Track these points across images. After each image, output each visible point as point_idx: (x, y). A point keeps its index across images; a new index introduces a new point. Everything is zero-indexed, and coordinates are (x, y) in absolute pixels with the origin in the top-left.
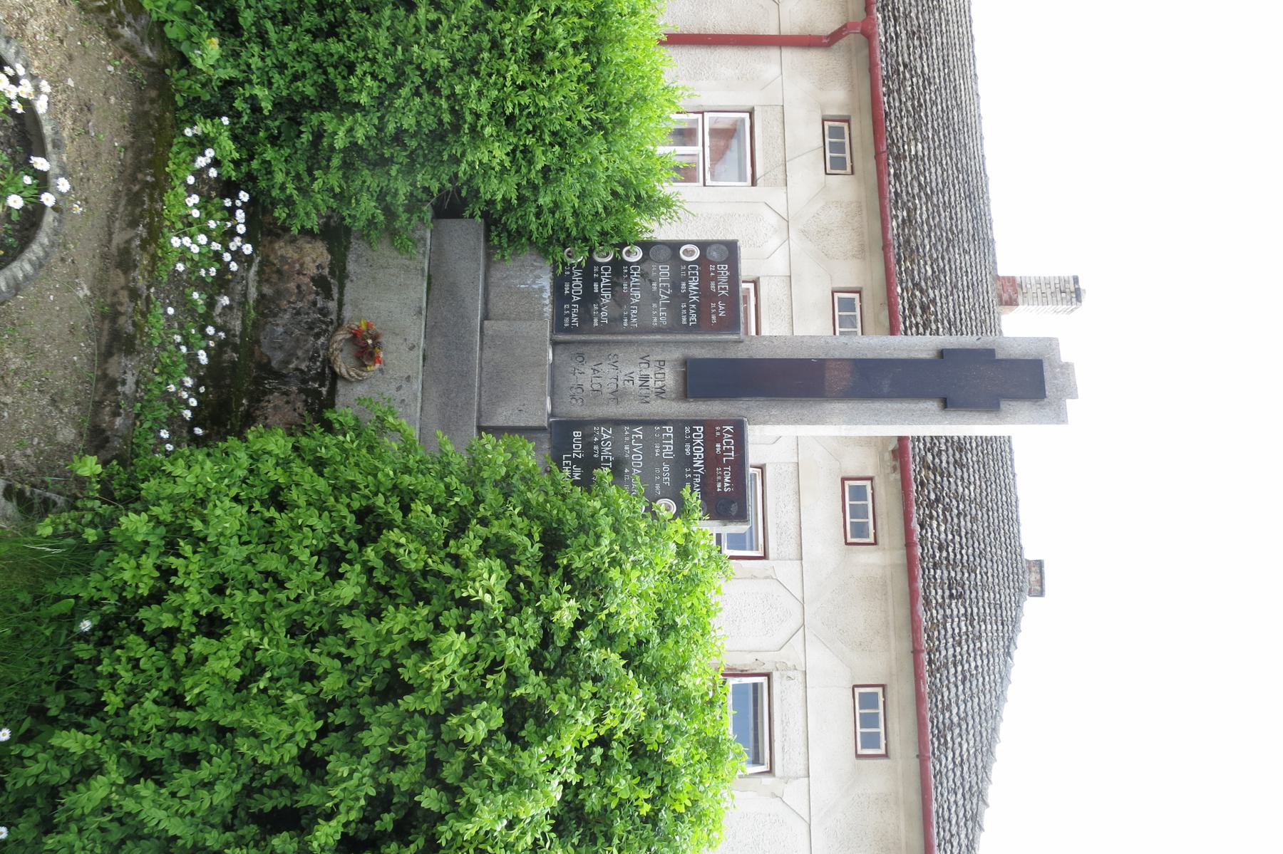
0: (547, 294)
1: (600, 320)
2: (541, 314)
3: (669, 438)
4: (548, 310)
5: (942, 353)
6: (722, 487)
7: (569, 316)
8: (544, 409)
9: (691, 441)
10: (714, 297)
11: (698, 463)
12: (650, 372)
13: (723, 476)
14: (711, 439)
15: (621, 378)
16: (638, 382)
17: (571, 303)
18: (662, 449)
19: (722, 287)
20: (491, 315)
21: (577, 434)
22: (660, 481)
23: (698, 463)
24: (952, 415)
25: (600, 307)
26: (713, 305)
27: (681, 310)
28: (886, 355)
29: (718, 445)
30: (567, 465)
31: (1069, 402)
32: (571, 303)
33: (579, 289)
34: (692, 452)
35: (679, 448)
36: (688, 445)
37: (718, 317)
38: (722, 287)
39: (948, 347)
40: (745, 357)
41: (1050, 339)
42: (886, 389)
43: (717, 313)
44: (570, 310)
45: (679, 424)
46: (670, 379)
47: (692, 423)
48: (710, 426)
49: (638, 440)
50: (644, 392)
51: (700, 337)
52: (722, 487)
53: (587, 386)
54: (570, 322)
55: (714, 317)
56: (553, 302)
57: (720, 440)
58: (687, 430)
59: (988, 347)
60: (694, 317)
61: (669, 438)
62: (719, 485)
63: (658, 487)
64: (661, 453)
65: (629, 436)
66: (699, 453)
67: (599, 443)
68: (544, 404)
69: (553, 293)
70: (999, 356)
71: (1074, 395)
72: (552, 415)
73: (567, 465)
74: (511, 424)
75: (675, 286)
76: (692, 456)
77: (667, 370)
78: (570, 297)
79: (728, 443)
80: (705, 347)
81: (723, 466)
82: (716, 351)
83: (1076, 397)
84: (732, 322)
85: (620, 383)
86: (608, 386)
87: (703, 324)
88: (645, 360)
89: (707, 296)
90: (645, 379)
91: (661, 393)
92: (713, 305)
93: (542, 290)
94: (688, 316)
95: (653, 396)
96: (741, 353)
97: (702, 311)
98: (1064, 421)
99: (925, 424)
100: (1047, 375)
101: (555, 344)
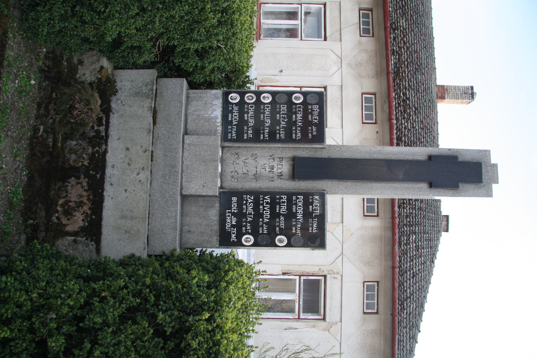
0: (219, 120)
1: (248, 135)
2: (216, 131)
3: (284, 202)
4: (220, 129)
5: (430, 157)
6: (312, 230)
7: (231, 132)
8: (216, 186)
9: (296, 204)
10: (311, 124)
11: (300, 216)
12: (275, 164)
13: (313, 224)
14: (307, 203)
15: (259, 167)
16: (268, 170)
17: (232, 126)
18: (280, 208)
19: (315, 118)
20: (188, 131)
21: (234, 199)
22: (279, 226)
23: (300, 216)
24: (434, 190)
25: (248, 128)
26: (310, 128)
27: (292, 130)
28: (402, 157)
29: (311, 207)
30: (229, 216)
31: (494, 186)
32: (232, 126)
33: (237, 118)
34: (296, 210)
35: (289, 208)
36: (294, 206)
37: (312, 135)
38: (315, 118)
39: (434, 154)
40: (327, 157)
41: (486, 151)
42: (401, 177)
43: (312, 133)
44: (231, 129)
45: (290, 195)
46: (285, 168)
47: (297, 194)
48: (307, 196)
49: (267, 203)
50: (271, 175)
51: (302, 146)
52: (312, 230)
53: (240, 171)
54: (232, 136)
55: (310, 135)
56: (222, 125)
57: (312, 204)
58: (294, 198)
59: (454, 154)
60: (299, 135)
61: (284, 202)
62: (310, 229)
63: (277, 229)
64: (280, 210)
65: (263, 200)
66: (300, 211)
67: (246, 204)
68: (216, 182)
69: (222, 119)
70: (460, 159)
71: (497, 182)
72: (221, 187)
73: (229, 216)
74: (198, 193)
75: (290, 118)
76: (297, 212)
77: (284, 163)
78: (231, 122)
79: (316, 206)
80: (305, 151)
81: (313, 218)
82: (310, 153)
83: (497, 183)
84: (320, 138)
85: (258, 170)
86: (252, 171)
87: (305, 139)
88: (272, 157)
89: (307, 123)
90: (272, 168)
91: (280, 175)
92: (310, 128)
93: (216, 118)
94: (296, 134)
95: (276, 177)
96: (324, 154)
97: (304, 131)
98: (491, 196)
99: (417, 192)
100: (484, 171)
101: (223, 148)
